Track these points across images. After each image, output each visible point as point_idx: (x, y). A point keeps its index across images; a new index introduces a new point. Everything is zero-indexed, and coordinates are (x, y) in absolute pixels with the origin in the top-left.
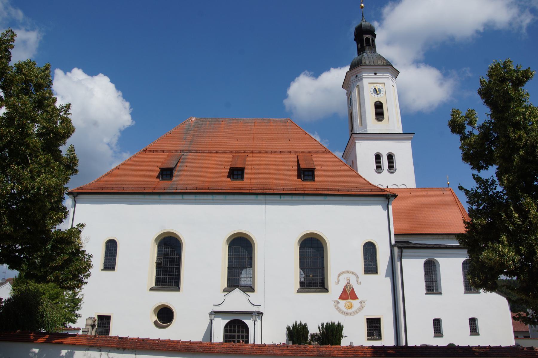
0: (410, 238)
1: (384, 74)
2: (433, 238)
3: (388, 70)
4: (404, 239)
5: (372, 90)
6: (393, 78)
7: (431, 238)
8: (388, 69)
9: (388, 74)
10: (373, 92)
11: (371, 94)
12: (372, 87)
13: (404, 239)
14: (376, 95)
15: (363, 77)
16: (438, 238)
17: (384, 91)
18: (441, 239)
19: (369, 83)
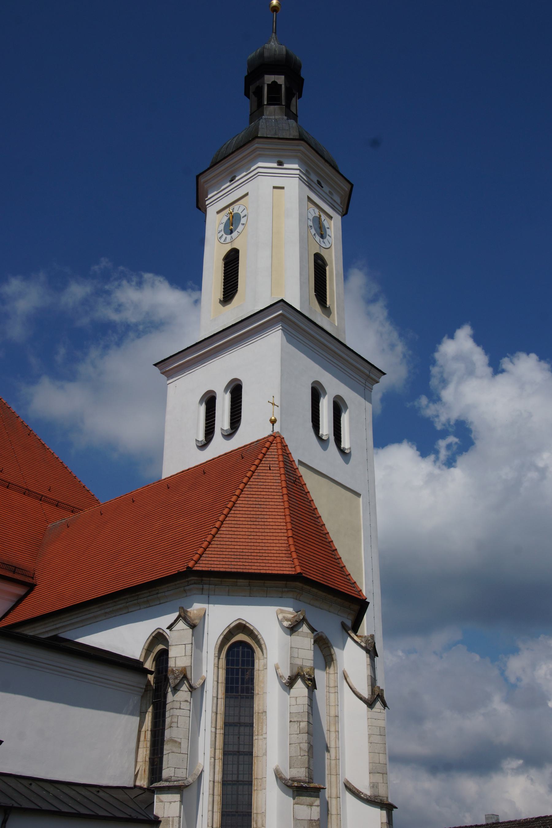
0: (58, 626)
1: (250, 168)
2: (103, 611)
3: (258, 152)
4: (47, 632)
5: (222, 227)
6: (286, 166)
7: (99, 613)
8: (257, 148)
9: (260, 164)
10: (223, 233)
11: (220, 238)
12: (224, 218)
13: (47, 632)
14: (229, 237)
15: (207, 203)
16: (115, 608)
17: (245, 216)
18: (121, 609)
19: (218, 212)
